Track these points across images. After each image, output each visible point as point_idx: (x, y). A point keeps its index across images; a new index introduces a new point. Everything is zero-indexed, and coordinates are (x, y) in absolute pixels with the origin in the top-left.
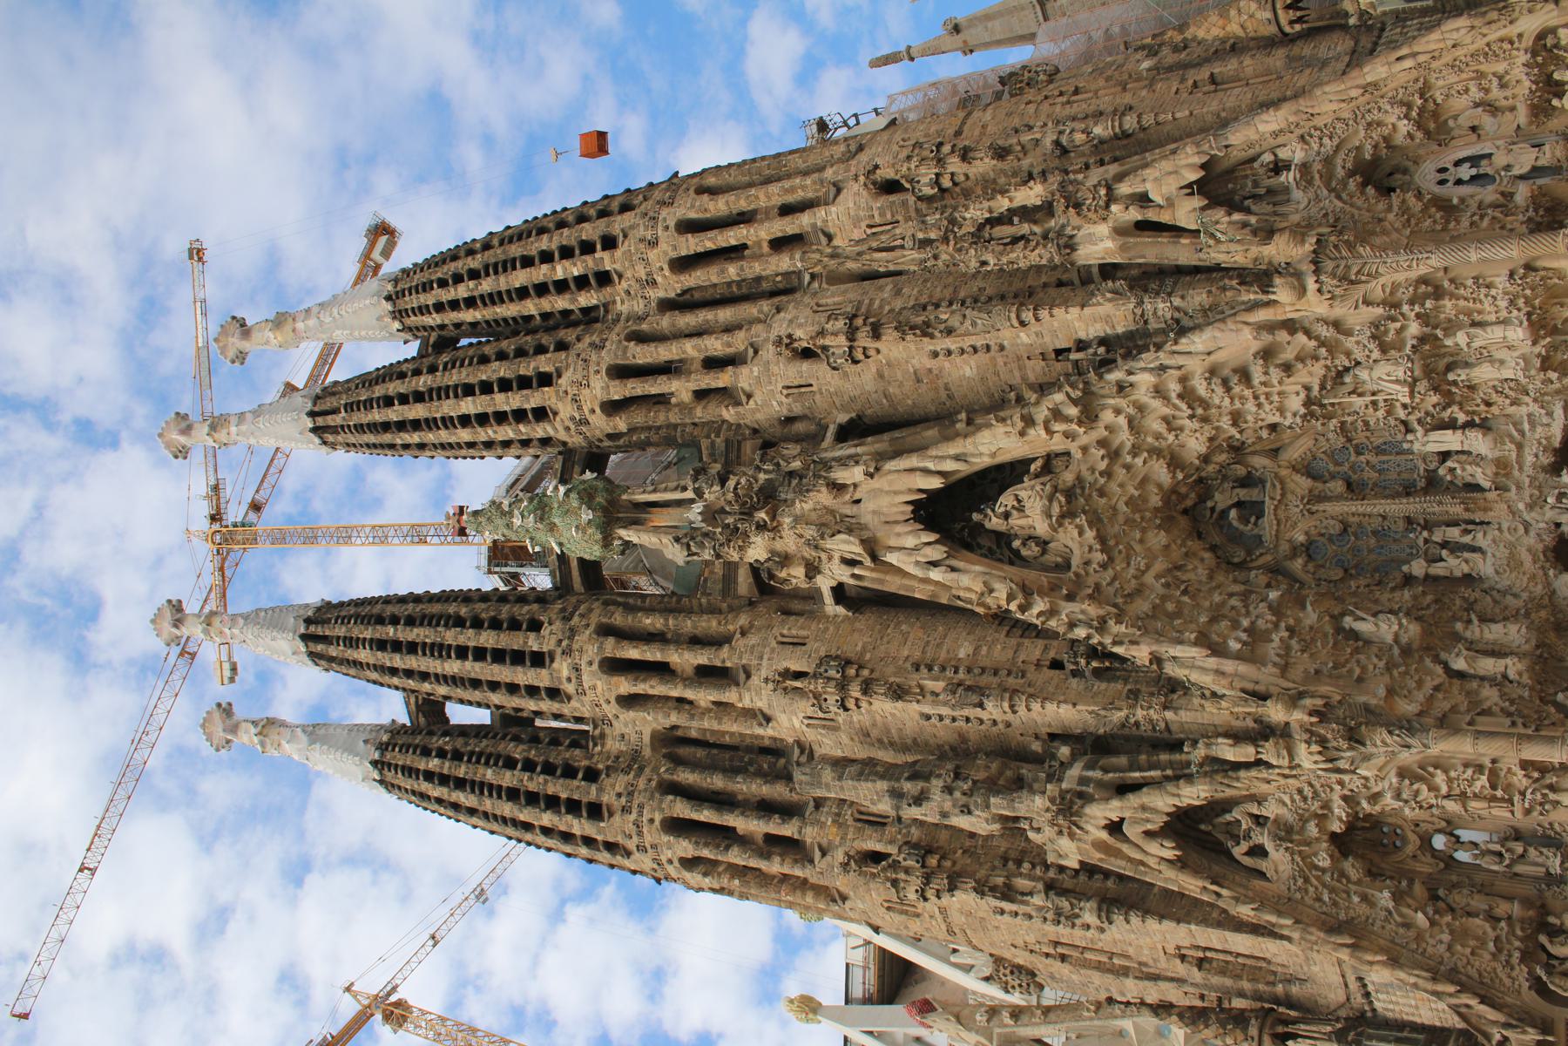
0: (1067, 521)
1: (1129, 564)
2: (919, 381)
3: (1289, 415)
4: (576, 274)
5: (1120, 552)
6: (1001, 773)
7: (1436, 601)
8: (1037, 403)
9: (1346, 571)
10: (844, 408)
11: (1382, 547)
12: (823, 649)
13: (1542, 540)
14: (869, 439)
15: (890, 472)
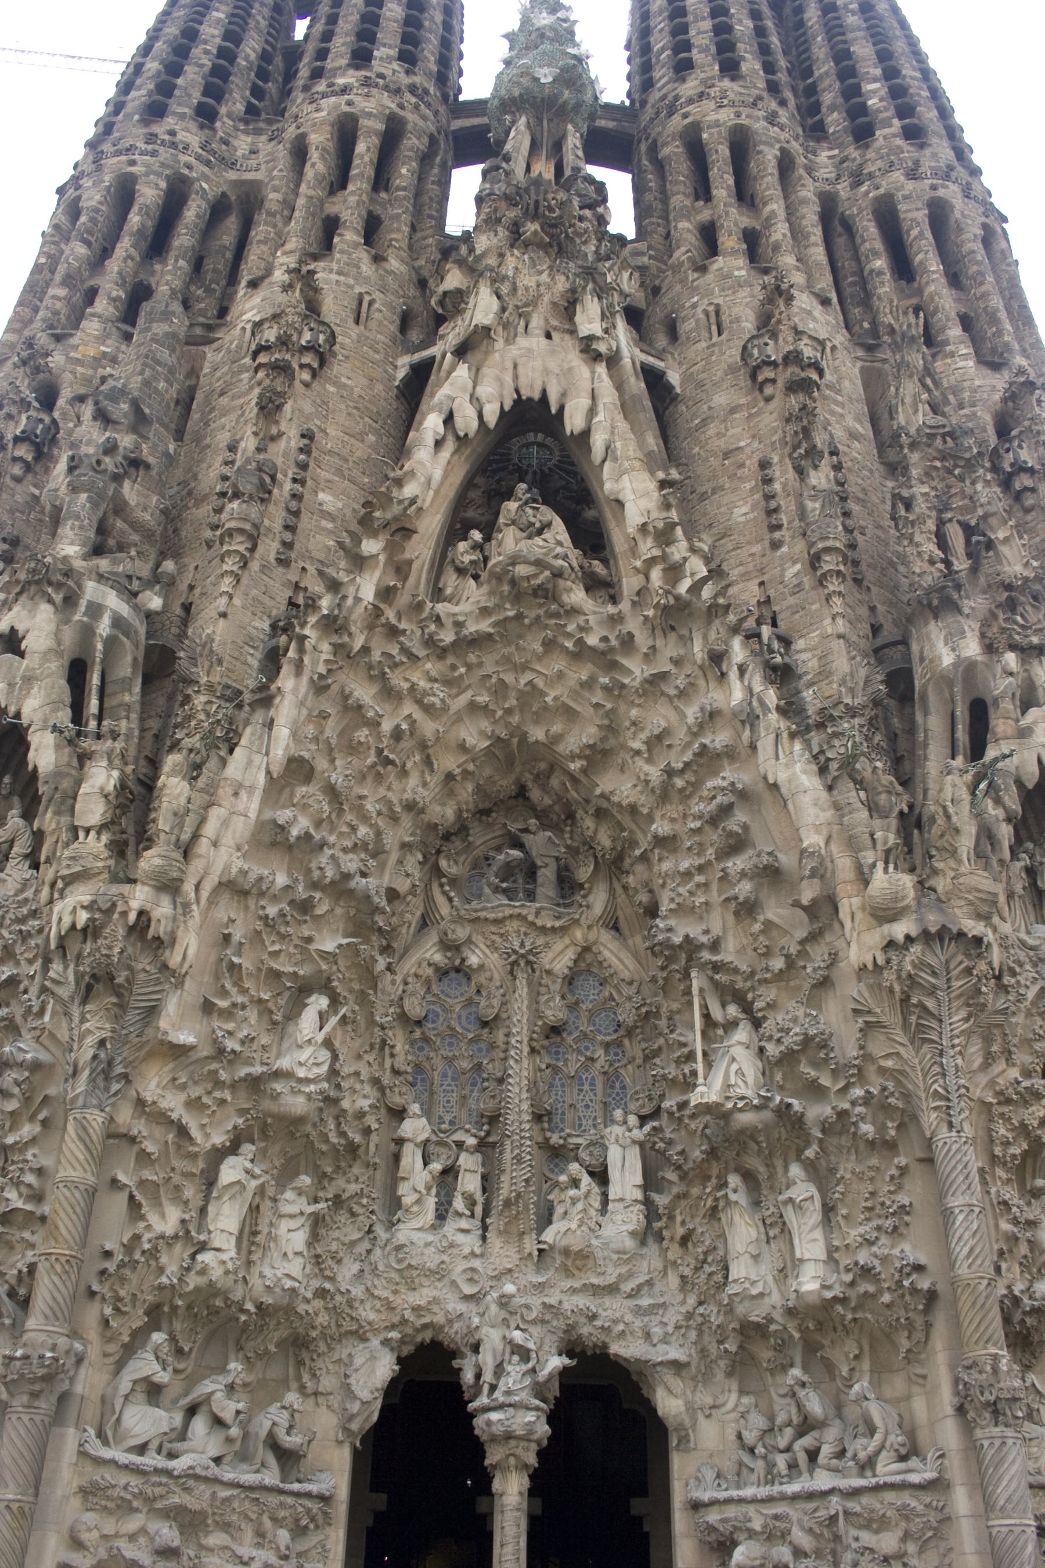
0: (506, 588)
1: (436, 680)
2: (726, 455)
3: (672, 922)
4: (870, 103)
5: (454, 668)
6: (136, 526)
7: (353, 1149)
8: (693, 550)
9: (419, 1023)
10: (686, 378)
11: (453, 1079)
12: (347, 341)
13: (450, 1322)
14: (643, 385)
15: (593, 372)
